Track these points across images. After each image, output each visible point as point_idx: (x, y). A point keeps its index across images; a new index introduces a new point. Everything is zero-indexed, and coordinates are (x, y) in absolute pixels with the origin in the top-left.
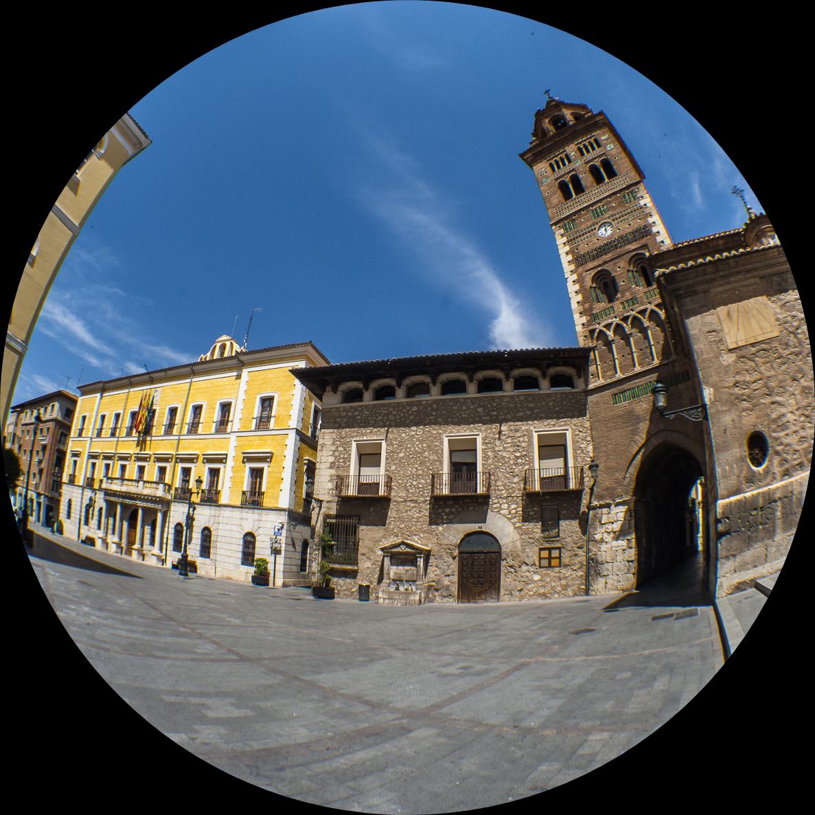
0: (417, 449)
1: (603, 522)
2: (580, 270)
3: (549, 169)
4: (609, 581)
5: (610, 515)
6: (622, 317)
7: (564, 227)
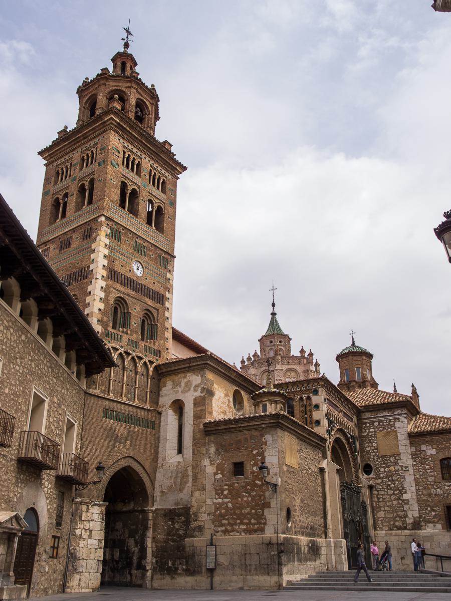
0: (17, 390)
1: (83, 519)
2: (110, 282)
3: (122, 156)
4: (83, 578)
5: (88, 514)
6: (126, 351)
7: (112, 229)
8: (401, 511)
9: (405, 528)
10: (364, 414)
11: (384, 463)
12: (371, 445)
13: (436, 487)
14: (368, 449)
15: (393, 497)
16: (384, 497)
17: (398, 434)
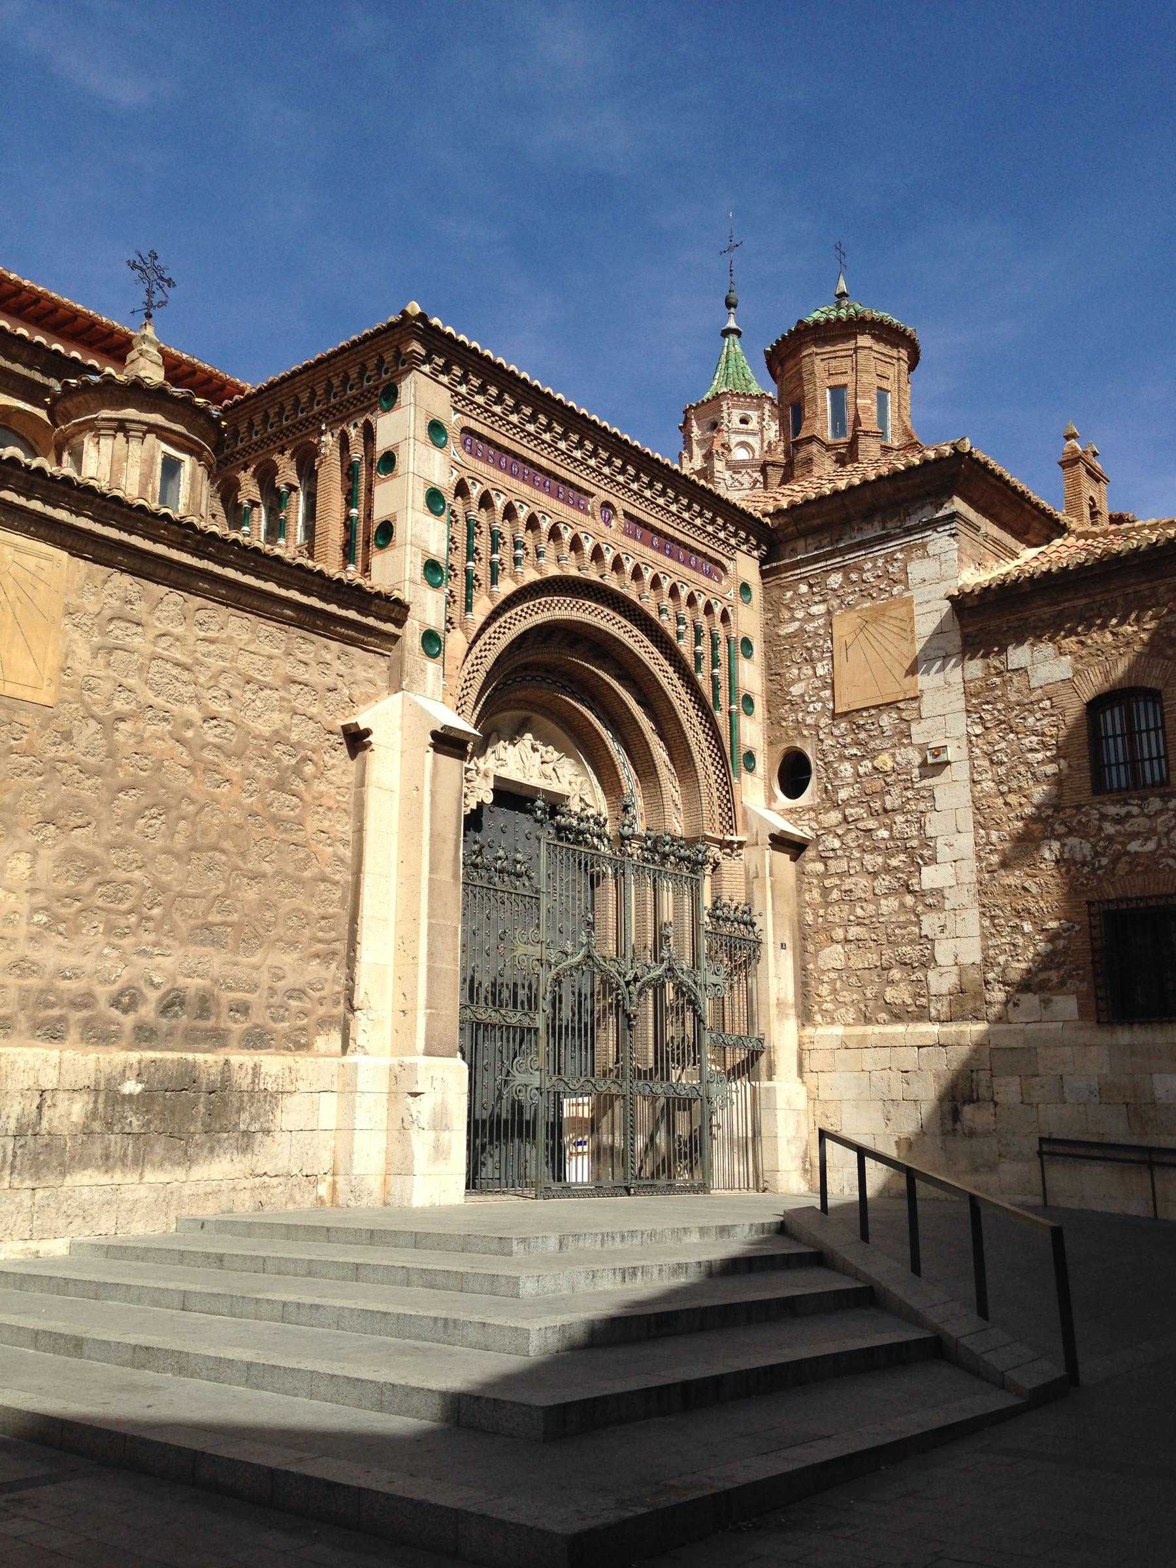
8: (912, 942)
9: (921, 1015)
10: (790, 547)
11: (858, 743)
12: (810, 672)
13: (1061, 829)
14: (796, 690)
15: (884, 882)
16: (848, 883)
17: (917, 610)
